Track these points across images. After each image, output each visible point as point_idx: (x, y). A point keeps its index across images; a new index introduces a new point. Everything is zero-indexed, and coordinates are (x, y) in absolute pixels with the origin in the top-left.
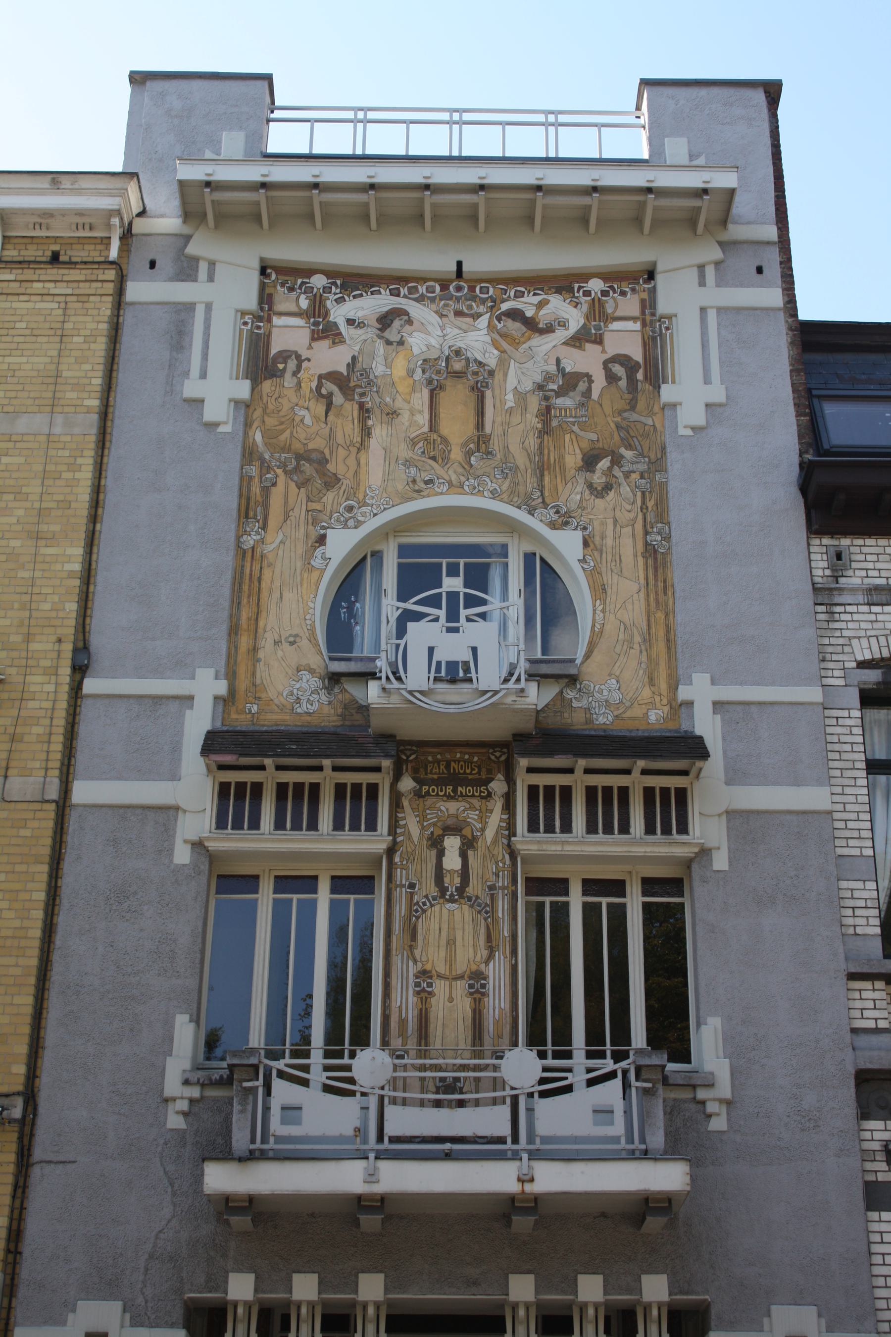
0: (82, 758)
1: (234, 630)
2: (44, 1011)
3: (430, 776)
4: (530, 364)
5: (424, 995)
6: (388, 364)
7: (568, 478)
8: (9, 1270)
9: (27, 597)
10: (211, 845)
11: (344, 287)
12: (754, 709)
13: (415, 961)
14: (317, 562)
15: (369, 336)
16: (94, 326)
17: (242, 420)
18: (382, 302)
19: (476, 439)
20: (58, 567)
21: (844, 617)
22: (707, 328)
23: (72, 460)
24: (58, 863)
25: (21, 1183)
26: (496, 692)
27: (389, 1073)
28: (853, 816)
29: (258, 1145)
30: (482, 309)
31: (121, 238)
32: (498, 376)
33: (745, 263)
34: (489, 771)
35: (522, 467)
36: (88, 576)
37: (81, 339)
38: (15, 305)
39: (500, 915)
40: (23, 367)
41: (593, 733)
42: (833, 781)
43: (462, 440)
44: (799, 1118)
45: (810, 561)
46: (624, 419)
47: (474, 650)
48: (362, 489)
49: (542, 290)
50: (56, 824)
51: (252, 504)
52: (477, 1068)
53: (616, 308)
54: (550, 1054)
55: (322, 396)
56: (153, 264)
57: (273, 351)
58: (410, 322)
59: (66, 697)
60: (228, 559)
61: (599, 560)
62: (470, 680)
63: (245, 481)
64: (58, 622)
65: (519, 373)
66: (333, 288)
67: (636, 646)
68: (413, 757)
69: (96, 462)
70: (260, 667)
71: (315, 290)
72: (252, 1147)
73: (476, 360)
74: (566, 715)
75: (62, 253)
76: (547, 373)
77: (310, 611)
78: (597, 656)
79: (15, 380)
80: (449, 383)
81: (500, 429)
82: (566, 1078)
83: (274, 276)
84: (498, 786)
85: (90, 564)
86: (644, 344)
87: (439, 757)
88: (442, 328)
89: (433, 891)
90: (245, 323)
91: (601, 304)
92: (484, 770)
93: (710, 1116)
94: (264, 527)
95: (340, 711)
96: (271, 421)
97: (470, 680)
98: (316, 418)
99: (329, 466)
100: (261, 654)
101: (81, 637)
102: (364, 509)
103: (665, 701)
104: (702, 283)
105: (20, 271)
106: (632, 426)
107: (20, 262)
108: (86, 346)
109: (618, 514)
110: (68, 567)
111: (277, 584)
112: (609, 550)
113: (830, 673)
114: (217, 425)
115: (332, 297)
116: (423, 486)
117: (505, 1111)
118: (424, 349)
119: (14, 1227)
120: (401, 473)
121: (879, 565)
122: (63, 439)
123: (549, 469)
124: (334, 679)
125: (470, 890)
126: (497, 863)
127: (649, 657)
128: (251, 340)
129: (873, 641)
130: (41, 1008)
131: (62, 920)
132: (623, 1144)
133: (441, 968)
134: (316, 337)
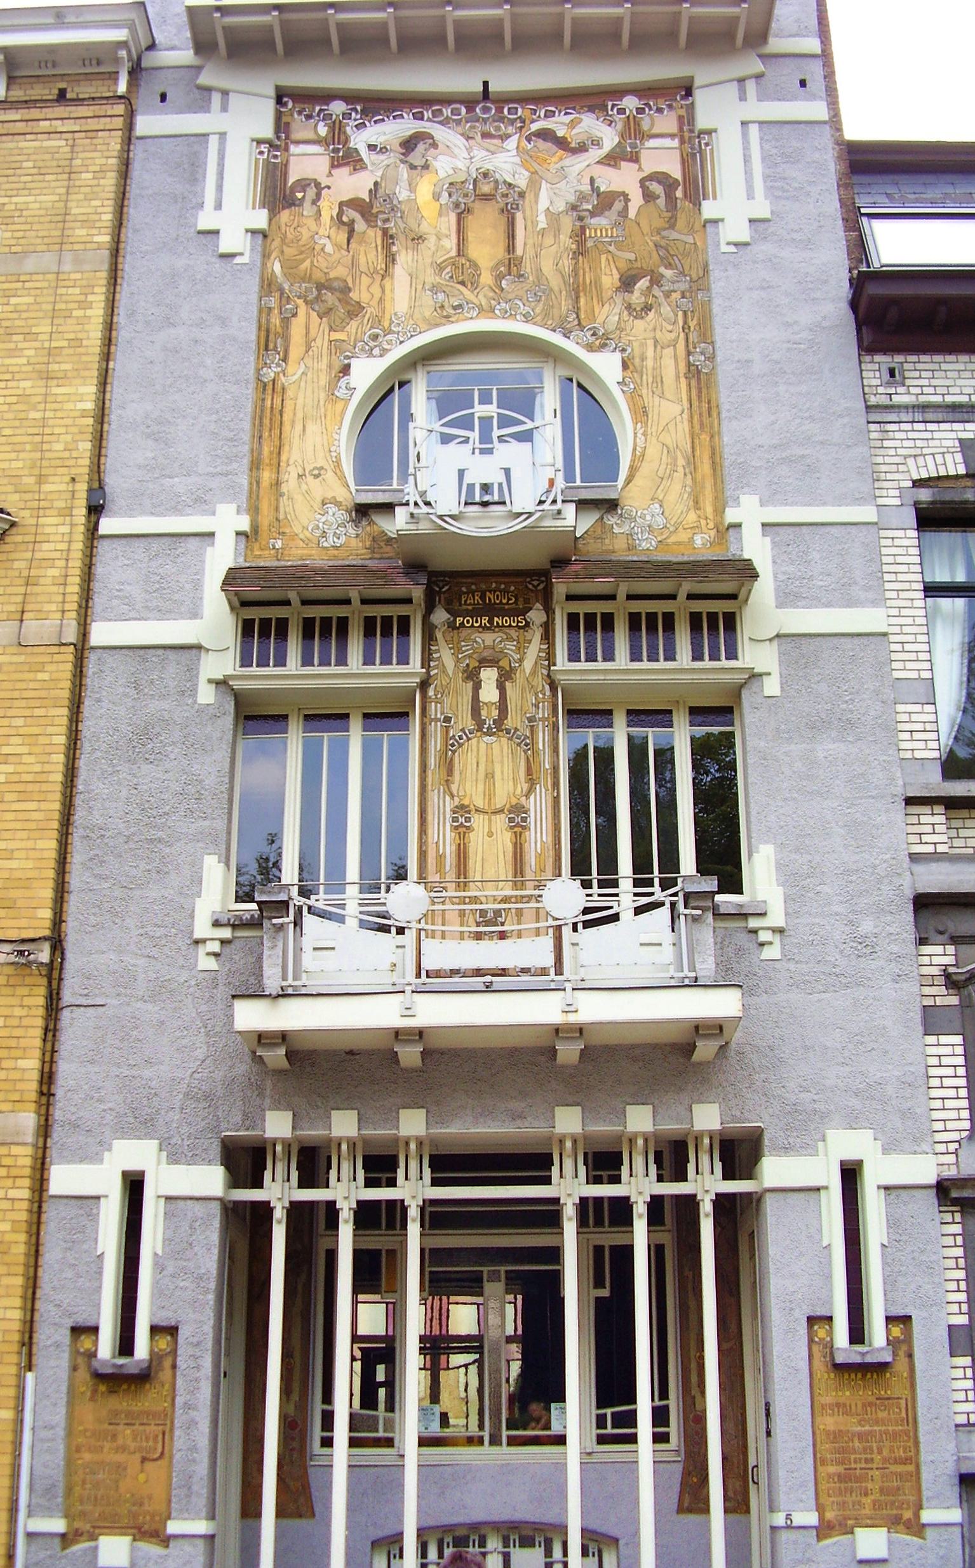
0: (99, 602)
1: (256, 465)
2: (69, 856)
3: (464, 607)
4: (562, 185)
5: (462, 830)
6: (412, 188)
7: (605, 300)
8: (43, 1111)
9: (38, 439)
10: (236, 684)
11: (364, 112)
12: (804, 529)
13: (452, 796)
14: (341, 393)
15: (392, 160)
16: (103, 161)
17: (260, 249)
18: (403, 126)
19: (507, 262)
20: (70, 406)
21: (898, 435)
22: (749, 143)
23: (82, 298)
24: (78, 707)
25: (51, 1027)
26: (530, 514)
27: (424, 906)
28: (911, 638)
29: (290, 981)
30: (510, 130)
31: (129, 72)
32: (529, 197)
33: (789, 74)
34: (527, 601)
35: (556, 289)
36: (101, 415)
37: (90, 176)
38: (22, 144)
39: (541, 747)
40: (31, 206)
41: (635, 559)
42: (889, 603)
43: (492, 264)
44: (855, 945)
45: (862, 378)
46: (663, 238)
47: (507, 472)
48: (387, 316)
49: (574, 109)
50: (75, 667)
51: (272, 337)
52: (520, 899)
53: (653, 125)
54: (595, 883)
55: (344, 223)
56: (163, 97)
57: (291, 181)
58: (435, 145)
59: (81, 537)
60: (249, 392)
61: (639, 381)
62: (504, 503)
63: (264, 311)
64: (72, 462)
65: (551, 193)
66: (353, 114)
67: (680, 469)
68: (446, 588)
69: (107, 299)
70: (284, 501)
71: (334, 117)
72: (284, 983)
73: (505, 182)
74: (607, 541)
75: (69, 90)
76: (581, 192)
77: (336, 443)
78: (638, 481)
79: (22, 220)
80: (477, 206)
81: (532, 253)
82: (611, 908)
83: (290, 105)
84: (537, 615)
85: (104, 403)
86: (683, 162)
87: (473, 587)
88: (469, 150)
89: (470, 724)
90: (261, 153)
91: (637, 123)
92: (521, 599)
93: (762, 945)
94: (285, 360)
95: (368, 544)
96: (289, 251)
97: (504, 503)
98: (337, 246)
99: (351, 295)
100: (284, 488)
101: (96, 477)
102: (389, 337)
103: (711, 525)
104: (743, 98)
105: (26, 111)
106: (672, 244)
107: (26, 102)
108: (95, 182)
109: (659, 335)
110: (80, 406)
111: (300, 415)
112: (650, 372)
113: (884, 493)
114: (233, 256)
115: (352, 123)
116: (453, 312)
117: (548, 942)
118: (451, 172)
119: (46, 1069)
120: (427, 300)
121: (934, 382)
122: (73, 276)
123: (584, 290)
124: (363, 511)
125: (509, 723)
126: (536, 694)
127: (694, 480)
128: (268, 170)
129: (929, 459)
130: (66, 853)
131: (82, 763)
132: (672, 971)
133: (480, 803)
134: (335, 164)
